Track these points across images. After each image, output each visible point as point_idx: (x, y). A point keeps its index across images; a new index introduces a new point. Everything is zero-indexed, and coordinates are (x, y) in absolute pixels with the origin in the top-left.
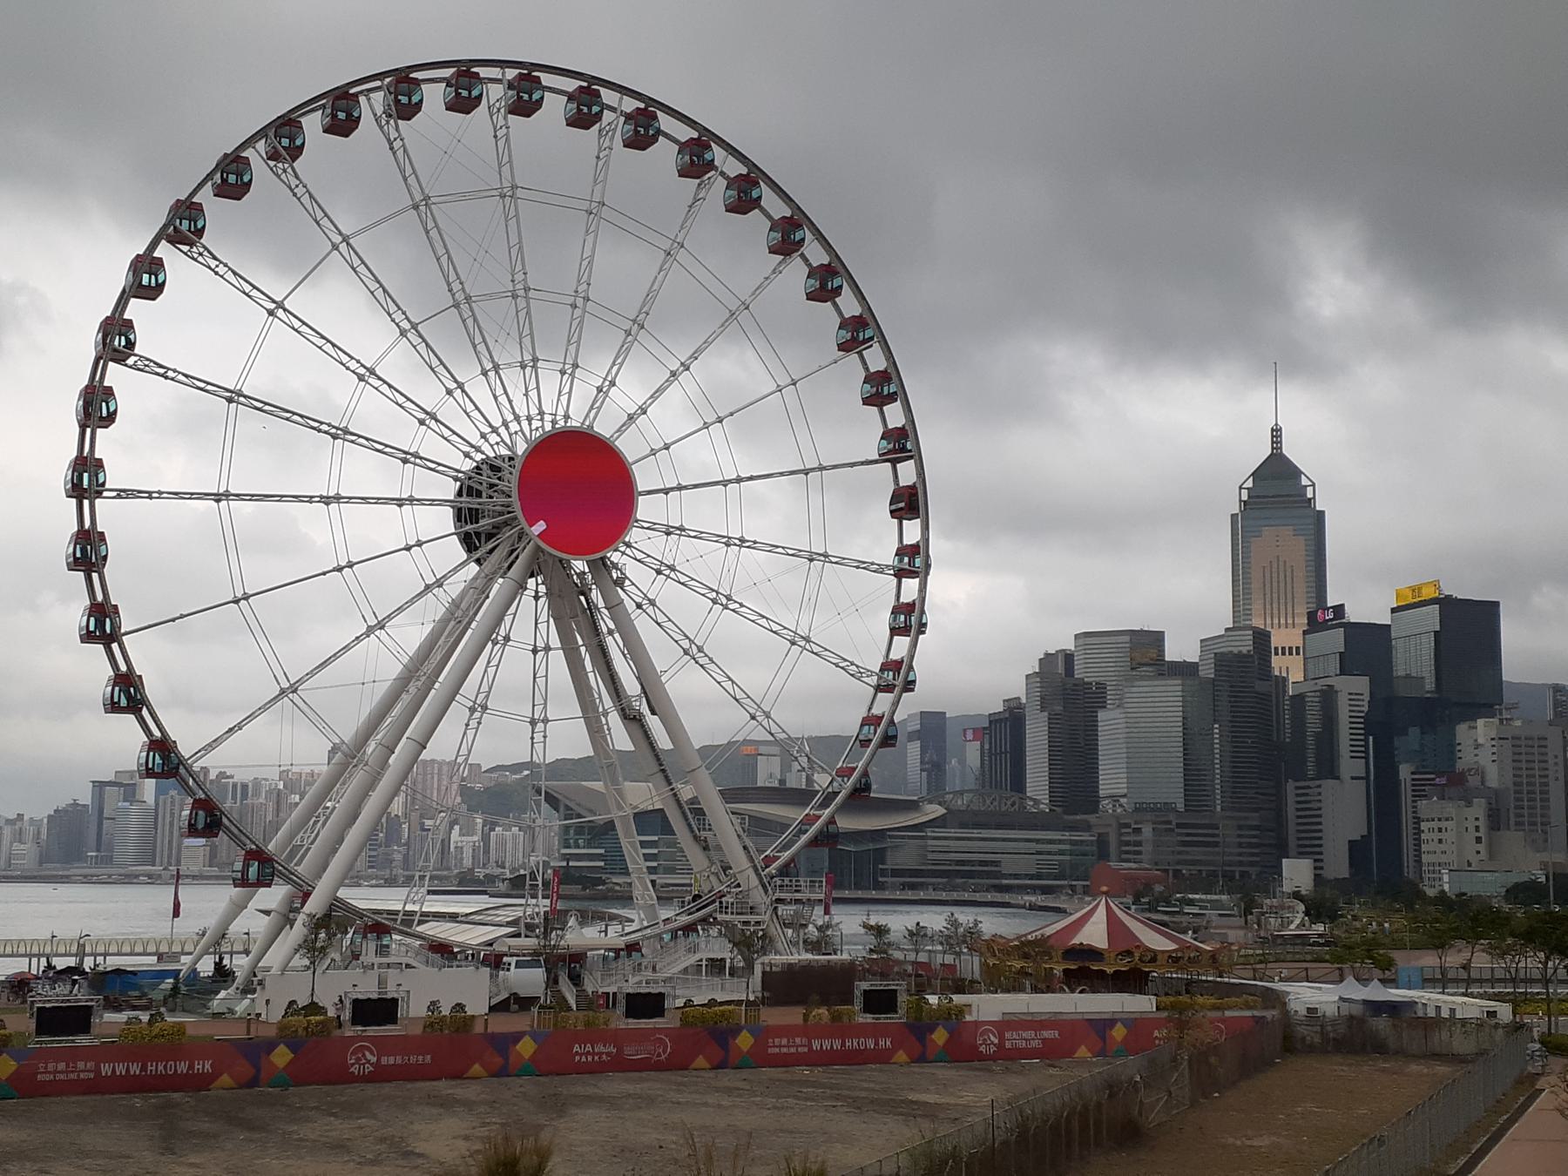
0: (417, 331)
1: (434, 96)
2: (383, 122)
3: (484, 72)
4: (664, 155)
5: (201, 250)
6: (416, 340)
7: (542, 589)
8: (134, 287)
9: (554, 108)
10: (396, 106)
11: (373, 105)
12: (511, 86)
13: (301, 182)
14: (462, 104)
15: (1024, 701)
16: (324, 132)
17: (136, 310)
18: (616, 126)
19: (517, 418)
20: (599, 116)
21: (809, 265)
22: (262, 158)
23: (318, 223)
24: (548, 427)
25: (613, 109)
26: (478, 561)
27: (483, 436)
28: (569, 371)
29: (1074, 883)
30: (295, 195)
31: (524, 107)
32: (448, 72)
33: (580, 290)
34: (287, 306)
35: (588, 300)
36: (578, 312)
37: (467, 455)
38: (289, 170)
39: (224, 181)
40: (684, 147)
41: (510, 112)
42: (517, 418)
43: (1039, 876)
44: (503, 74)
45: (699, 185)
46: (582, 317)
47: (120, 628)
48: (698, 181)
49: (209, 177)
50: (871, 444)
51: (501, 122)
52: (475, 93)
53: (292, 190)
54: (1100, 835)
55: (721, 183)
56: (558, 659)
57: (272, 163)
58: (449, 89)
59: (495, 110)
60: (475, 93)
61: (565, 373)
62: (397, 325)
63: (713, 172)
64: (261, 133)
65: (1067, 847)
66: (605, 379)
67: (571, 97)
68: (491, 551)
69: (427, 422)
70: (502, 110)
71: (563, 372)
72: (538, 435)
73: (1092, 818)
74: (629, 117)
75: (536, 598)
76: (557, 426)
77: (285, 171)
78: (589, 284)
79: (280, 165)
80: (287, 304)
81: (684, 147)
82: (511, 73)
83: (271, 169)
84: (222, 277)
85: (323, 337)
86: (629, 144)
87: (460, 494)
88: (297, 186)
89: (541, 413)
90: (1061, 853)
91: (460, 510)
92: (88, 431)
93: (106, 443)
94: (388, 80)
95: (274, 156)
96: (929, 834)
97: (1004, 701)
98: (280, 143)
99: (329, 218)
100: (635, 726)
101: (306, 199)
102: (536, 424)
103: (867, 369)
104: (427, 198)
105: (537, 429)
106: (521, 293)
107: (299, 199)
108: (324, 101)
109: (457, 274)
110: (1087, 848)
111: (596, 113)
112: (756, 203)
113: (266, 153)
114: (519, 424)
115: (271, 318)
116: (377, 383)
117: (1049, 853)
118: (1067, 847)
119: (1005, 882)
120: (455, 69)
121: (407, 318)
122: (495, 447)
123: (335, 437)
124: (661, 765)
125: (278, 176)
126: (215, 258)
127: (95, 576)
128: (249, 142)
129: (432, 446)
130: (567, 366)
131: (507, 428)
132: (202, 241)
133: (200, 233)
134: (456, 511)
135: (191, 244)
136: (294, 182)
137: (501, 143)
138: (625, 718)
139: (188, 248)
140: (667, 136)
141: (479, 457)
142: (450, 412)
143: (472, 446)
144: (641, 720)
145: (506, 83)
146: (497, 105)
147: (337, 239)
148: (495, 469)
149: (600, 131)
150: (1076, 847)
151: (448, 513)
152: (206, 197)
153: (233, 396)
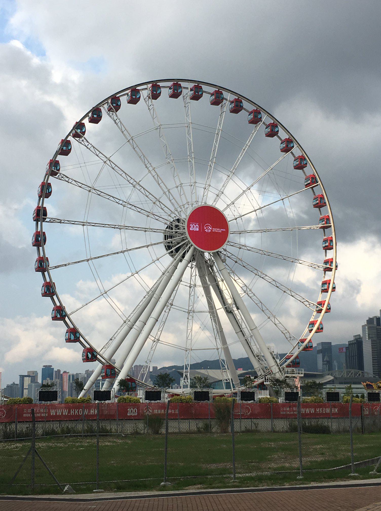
1: (165, 93)
2: (147, 100)
5: (83, 139)
8: (60, 150)
11: (144, 94)
14: (175, 95)
15: (361, 336)
17: (60, 158)
21: (294, 157)
31: (196, 97)
38: (114, 114)
39: (93, 116)
45: (256, 127)
47: (49, 266)
48: (255, 125)
52: (179, 91)
56: (200, 290)
57: (109, 112)
60: (179, 91)
67: (212, 95)
74: (232, 102)
75: (192, 268)
77: (113, 114)
79: (111, 113)
84: (89, 149)
87: (167, 228)
88: (116, 120)
91: (165, 236)
92: (42, 199)
93: (48, 204)
95: (110, 110)
97: (354, 336)
98: (112, 105)
100: (230, 315)
113: (108, 109)
120: (151, 84)
124: (240, 329)
127: (41, 248)
129: (157, 210)
131: (177, 210)
133: (84, 133)
135: (79, 137)
136: (115, 118)
138: (227, 312)
140: (245, 109)
149: (221, 106)
151: (162, 236)
152: (86, 121)
153: (91, 189)
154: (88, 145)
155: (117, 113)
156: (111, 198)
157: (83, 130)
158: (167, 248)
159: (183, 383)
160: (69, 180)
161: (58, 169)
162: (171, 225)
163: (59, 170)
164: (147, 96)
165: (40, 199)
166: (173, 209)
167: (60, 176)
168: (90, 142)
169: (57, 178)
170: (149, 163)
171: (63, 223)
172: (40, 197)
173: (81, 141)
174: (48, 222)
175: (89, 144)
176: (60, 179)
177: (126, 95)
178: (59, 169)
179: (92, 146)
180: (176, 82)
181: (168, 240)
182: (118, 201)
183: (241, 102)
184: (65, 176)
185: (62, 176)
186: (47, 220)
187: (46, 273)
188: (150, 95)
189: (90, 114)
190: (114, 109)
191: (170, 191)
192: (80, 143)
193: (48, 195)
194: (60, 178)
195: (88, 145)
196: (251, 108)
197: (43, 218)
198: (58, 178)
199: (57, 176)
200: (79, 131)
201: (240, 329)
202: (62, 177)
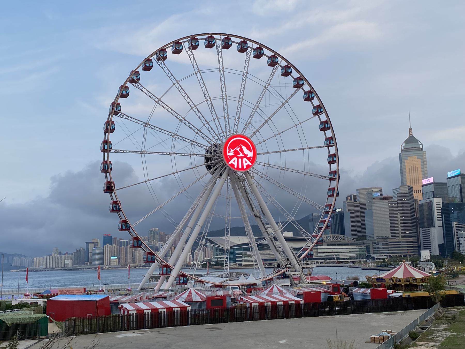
0: (196, 108)
1: (202, 44)
2: (188, 50)
3: (216, 37)
4: (264, 60)
5: (138, 84)
6: (195, 110)
7: (229, 180)
9: (234, 47)
10: (192, 46)
12: (223, 41)
13: (166, 66)
16: (173, 53)
18: (251, 52)
19: (223, 132)
20: (247, 49)
22: (155, 60)
23: (170, 78)
24: (231, 135)
25: (250, 48)
26: (212, 173)
27: (213, 137)
28: (237, 120)
29: (360, 260)
30: (163, 70)
31: (226, 46)
32: (206, 37)
33: (240, 97)
34: (161, 100)
35: (243, 99)
36: (240, 103)
37: (209, 142)
38: (163, 63)
39: (145, 65)
40: (269, 58)
41: (222, 48)
42: (223, 132)
43: (350, 259)
44: (221, 37)
45: (274, 68)
46: (241, 104)
48: (273, 67)
49: (141, 64)
50: (322, 142)
51: (220, 50)
52: (213, 43)
53: (163, 69)
54: (367, 246)
55: (280, 68)
57: (158, 61)
58: (206, 42)
59: (218, 47)
60: (213, 43)
61: (236, 120)
62: (190, 106)
63: (277, 65)
64: (155, 53)
65: (358, 250)
66: (247, 122)
67: (239, 44)
68: (215, 170)
69: (198, 133)
70: (220, 47)
71: (236, 120)
72: (229, 137)
73: (365, 241)
74: (255, 50)
75: (228, 183)
76: (238, 133)
77: (161, 63)
78: (243, 95)
79: (160, 62)
80: (161, 99)
81: (269, 58)
82: (223, 37)
83: (157, 63)
84: (144, 92)
85: (171, 109)
86: (255, 57)
88: (164, 67)
89: (230, 131)
90: (356, 252)
91: (206, 158)
94: (189, 39)
95: (159, 59)
96: (318, 248)
98: (161, 56)
99: (173, 76)
101: (167, 71)
102: (228, 134)
103: (320, 120)
104: (199, 71)
105: (228, 135)
106: (225, 97)
107: (165, 71)
108: (172, 44)
109: (207, 92)
110: (364, 250)
111: (246, 48)
112: (290, 74)
113: (157, 59)
114: (224, 134)
115: (157, 104)
116: (185, 122)
117: (353, 252)
118: (358, 250)
119: (340, 260)
121: (193, 104)
122: (217, 140)
123: (173, 137)
125: (159, 65)
126: (142, 87)
128: (152, 55)
130: (237, 118)
132: (139, 82)
133: (139, 79)
134: (205, 158)
135: (136, 82)
136: (164, 66)
137: (220, 56)
139: (135, 84)
141: (212, 143)
142: (205, 131)
143: (211, 140)
144: (259, 217)
145: (221, 40)
146: (219, 46)
147: (175, 82)
148: (216, 146)
149: (246, 53)
150: (360, 250)
151: (203, 158)
152: (140, 70)
154: (143, 89)
155: (164, 62)
156: (163, 131)
157: (138, 77)
158: (207, 167)
159: (224, 275)
160: (128, 118)
161: (119, 109)
162: (210, 150)
163: (120, 110)
164: (188, 48)
165: (105, 135)
166: (211, 138)
167: (121, 115)
168: (144, 87)
169: (118, 116)
170: (192, 102)
171: (125, 153)
172: (106, 132)
173: (137, 86)
174: (113, 152)
175: (144, 88)
176: (121, 117)
177: (171, 47)
178: (120, 109)
179: (146, 90)
180: (210, 36)
181: (209, 162)
182: (168, 133)
183: (262, 49)
184: (125, 115)
185: (123, 115)
186: (112, 151)
187: (113, 194)
188: (190, 47)
189: (143, 64)
190: (162, 59)
191: (209, 123)
192: (136, 87)
193: (112, 131)
194: (121, 116)
195: (143, 89)
196: (270, 54)
197: (109, 150)
198: (119, 116)
199: (119, 115)
200: (134, 78)
201: (266, 230)
202: (123, 116)
